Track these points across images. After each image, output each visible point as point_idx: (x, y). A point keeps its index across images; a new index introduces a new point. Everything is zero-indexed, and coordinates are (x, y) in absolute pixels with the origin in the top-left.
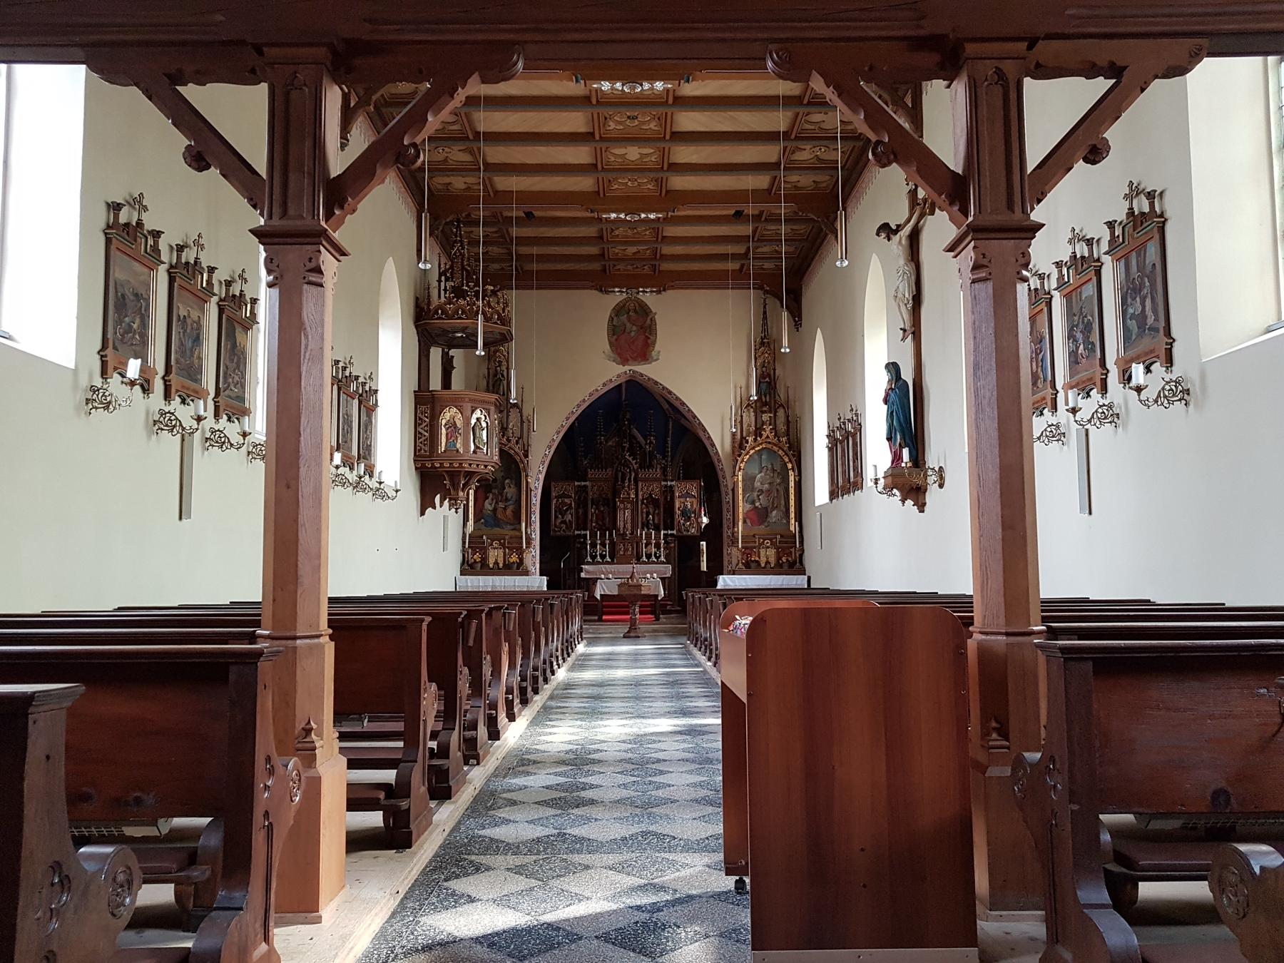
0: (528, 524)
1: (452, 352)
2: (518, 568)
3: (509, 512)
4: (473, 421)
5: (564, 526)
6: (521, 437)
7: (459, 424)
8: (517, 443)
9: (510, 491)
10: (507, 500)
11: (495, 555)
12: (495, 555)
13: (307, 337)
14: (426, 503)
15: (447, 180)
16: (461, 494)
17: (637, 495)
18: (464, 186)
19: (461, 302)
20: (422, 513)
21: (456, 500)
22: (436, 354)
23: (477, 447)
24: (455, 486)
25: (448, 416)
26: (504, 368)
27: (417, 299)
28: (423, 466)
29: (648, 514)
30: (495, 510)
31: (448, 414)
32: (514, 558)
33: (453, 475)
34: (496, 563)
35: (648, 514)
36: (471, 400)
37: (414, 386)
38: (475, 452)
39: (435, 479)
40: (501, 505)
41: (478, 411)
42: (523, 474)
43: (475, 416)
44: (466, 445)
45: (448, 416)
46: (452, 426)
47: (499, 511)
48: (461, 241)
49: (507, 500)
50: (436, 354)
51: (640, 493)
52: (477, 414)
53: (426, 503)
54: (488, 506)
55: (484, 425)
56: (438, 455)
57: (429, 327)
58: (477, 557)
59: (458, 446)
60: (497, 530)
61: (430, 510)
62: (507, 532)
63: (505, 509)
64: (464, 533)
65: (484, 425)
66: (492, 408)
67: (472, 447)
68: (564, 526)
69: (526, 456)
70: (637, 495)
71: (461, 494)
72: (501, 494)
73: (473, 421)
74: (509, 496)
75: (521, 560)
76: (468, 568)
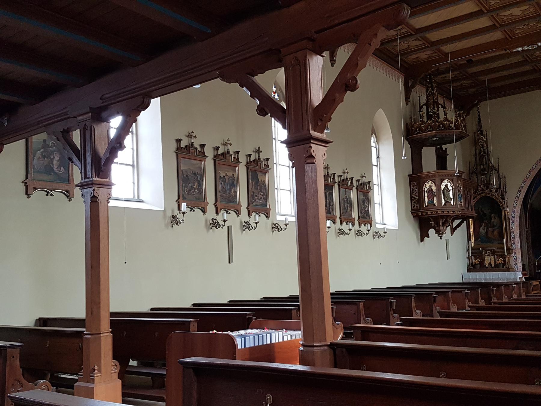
1: (444, 147)
2: (504, 267)
3: (496, 233)
6: (500, 187)
7: (434, 189)
8: (496, 191)
9: (495, 221)
10: (494, 226)
11: (489, 260)
12: (489, 260)
14: (423, 235)
15: (416, 56)
18: (427, 56)
19: (429, 122)
21: (439, 232)
23: (446, 202)
25: (427, 186)
27: (407, 124)
28: (417, 215)
30: (487, 233)
31: (429, 184)
32: (501, 261)
33: (436, 219)
34: (490, 264)
36: (440, 176)
38: (445, 204)
39: (426, 220)
40: (490, 229)
41: (446, 181)
42: (503, 210)
43: (444, 184)
44: (439, 201)
45: (427, 186)
46: (430, 190)
48: (432, 87)
49: (494, 226)
52: (445, 182)
53: (423, 235)
54: (482, 230)
55: (450, 188)
57: (414, 137)
58: (477, 261)
59: (435, 202)
62: (495, 245)
63: (493, 231)
64: (468, 247)
67: (443, 202)
69: (503, 199)
74: (495, 224)
75: (505, 261)
76: (472, 268)
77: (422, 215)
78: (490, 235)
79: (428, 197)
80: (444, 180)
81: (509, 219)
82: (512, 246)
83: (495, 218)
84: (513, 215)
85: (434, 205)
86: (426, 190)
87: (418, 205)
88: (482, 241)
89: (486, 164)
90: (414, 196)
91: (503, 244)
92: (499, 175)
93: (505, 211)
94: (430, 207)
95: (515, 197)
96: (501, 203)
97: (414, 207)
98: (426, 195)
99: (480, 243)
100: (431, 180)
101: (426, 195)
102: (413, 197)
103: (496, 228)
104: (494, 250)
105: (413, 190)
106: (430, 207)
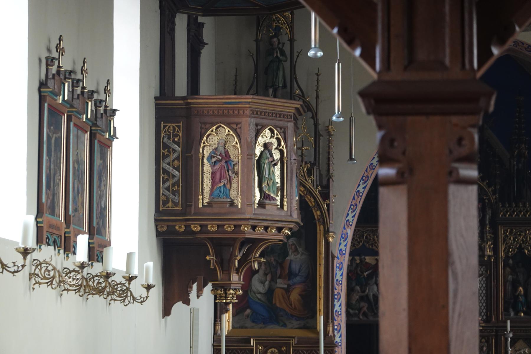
0: (329, 318)
3: (295, 296)
4: (258, 150)
5: (364, 306)
7: (235, 154)
13: (456, 278)
16: (235, 278)
17: (495, 250)
20: (166, 312)
22: (181, 23)
23: (265, 196)
24: (225, 265)
26: (285, 38)
28: (171, 231)
29: (515, 285)
30: (270, 293)
31: (217, 138)
33: (222, 246)
35: (515, 285)
36: (256, 113)
37: (155, 91)
38: (261, 205)
40: (281, 284)
42: (320, 229)
43: (261, 140)
44: (247, 193)
46: (223, 159)
47: (278, 294)
49: (291, 275)
50: (181, 23)
51: (502, 248)
52: (265, 137)
56: (198, 212)
59: (233, 194)
60: (274, 331)
61: (178, 307)
63: (288, 290)
65: (277, 156)
66: (290, 125)
68: (364, 306)
69: (326, 196)
70: (495, 250)
71: (235, 278)
72: (281, 265)
73: (258, 150)
74: (295, 267)
77: (188, 231)
78: (278, 301)
79: (213, 174)
80: (263, 127)
81: (333, 257)
82: (334, 336)
83: (296, 250)
84: (342, 247)
85: (232, 204)
86: (207, 152)
87: (178, 199)
88: (255, 319)
89: (285, 86)
90: (170, 169)
91: (314, 329)
92: (316, 125)
93: (327, 232)
94: (216, 209)
95: (354, 193)
96: (319, 207)
97: (165, 203)
98: (207, 168)
99: (249, 323)
100: (228, 125)
101: (207, 168)
102: (165, 171)
103: (298, 278)
104: (288, 345)
105: (166, 146)
106: (216, 209)
